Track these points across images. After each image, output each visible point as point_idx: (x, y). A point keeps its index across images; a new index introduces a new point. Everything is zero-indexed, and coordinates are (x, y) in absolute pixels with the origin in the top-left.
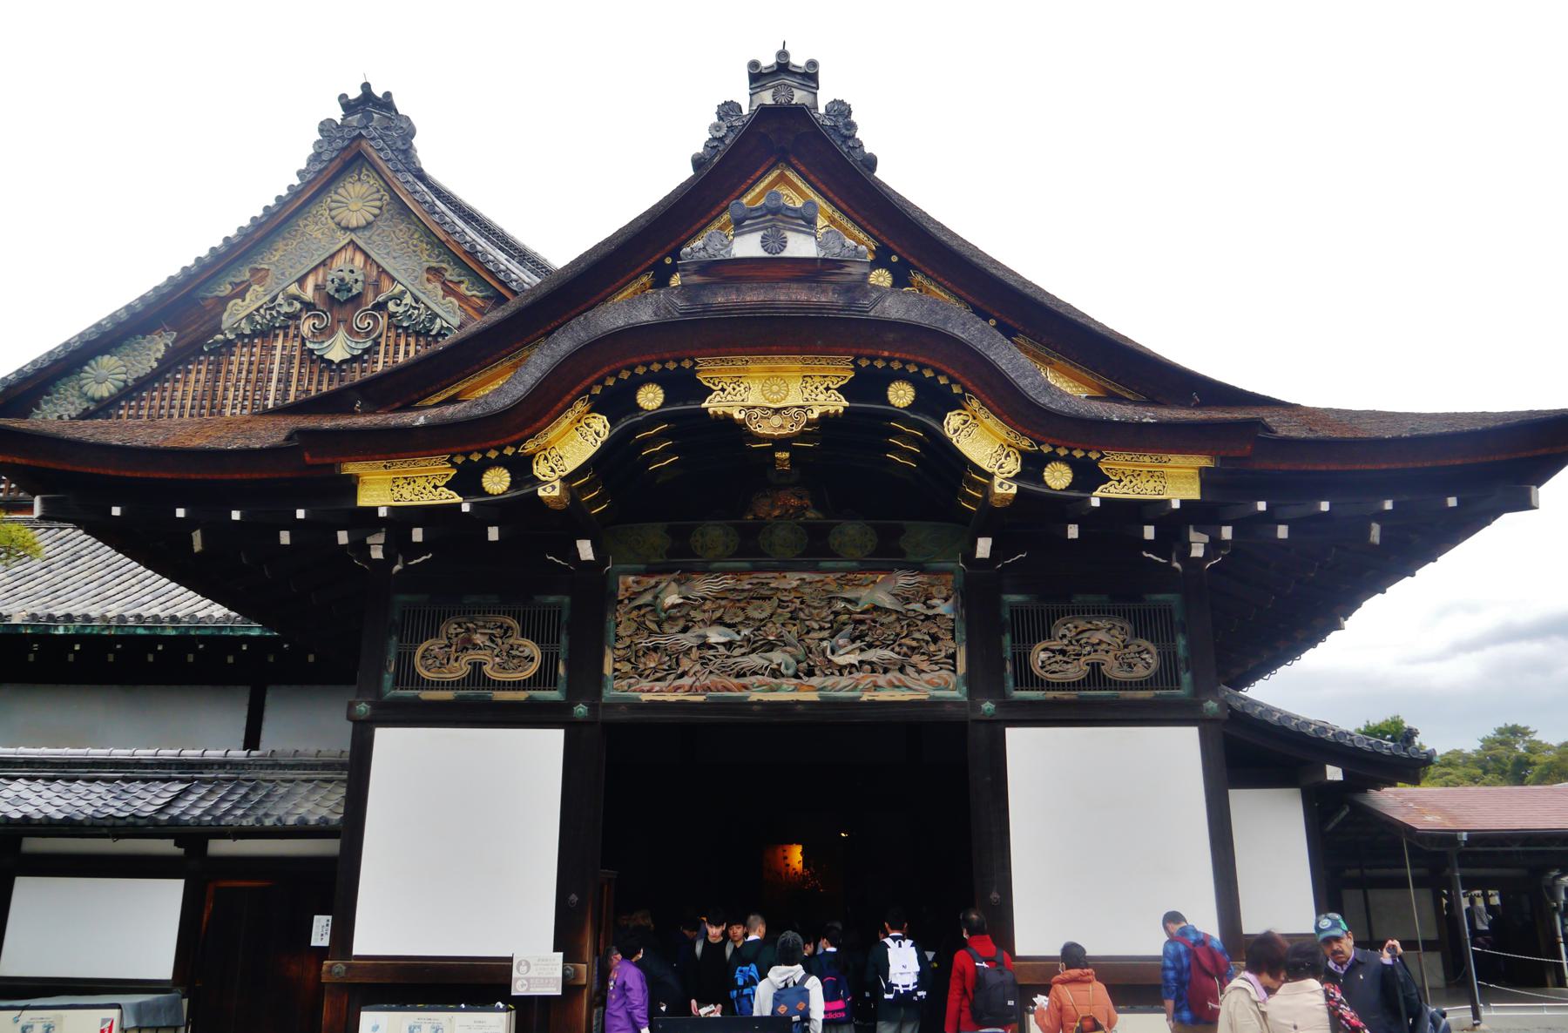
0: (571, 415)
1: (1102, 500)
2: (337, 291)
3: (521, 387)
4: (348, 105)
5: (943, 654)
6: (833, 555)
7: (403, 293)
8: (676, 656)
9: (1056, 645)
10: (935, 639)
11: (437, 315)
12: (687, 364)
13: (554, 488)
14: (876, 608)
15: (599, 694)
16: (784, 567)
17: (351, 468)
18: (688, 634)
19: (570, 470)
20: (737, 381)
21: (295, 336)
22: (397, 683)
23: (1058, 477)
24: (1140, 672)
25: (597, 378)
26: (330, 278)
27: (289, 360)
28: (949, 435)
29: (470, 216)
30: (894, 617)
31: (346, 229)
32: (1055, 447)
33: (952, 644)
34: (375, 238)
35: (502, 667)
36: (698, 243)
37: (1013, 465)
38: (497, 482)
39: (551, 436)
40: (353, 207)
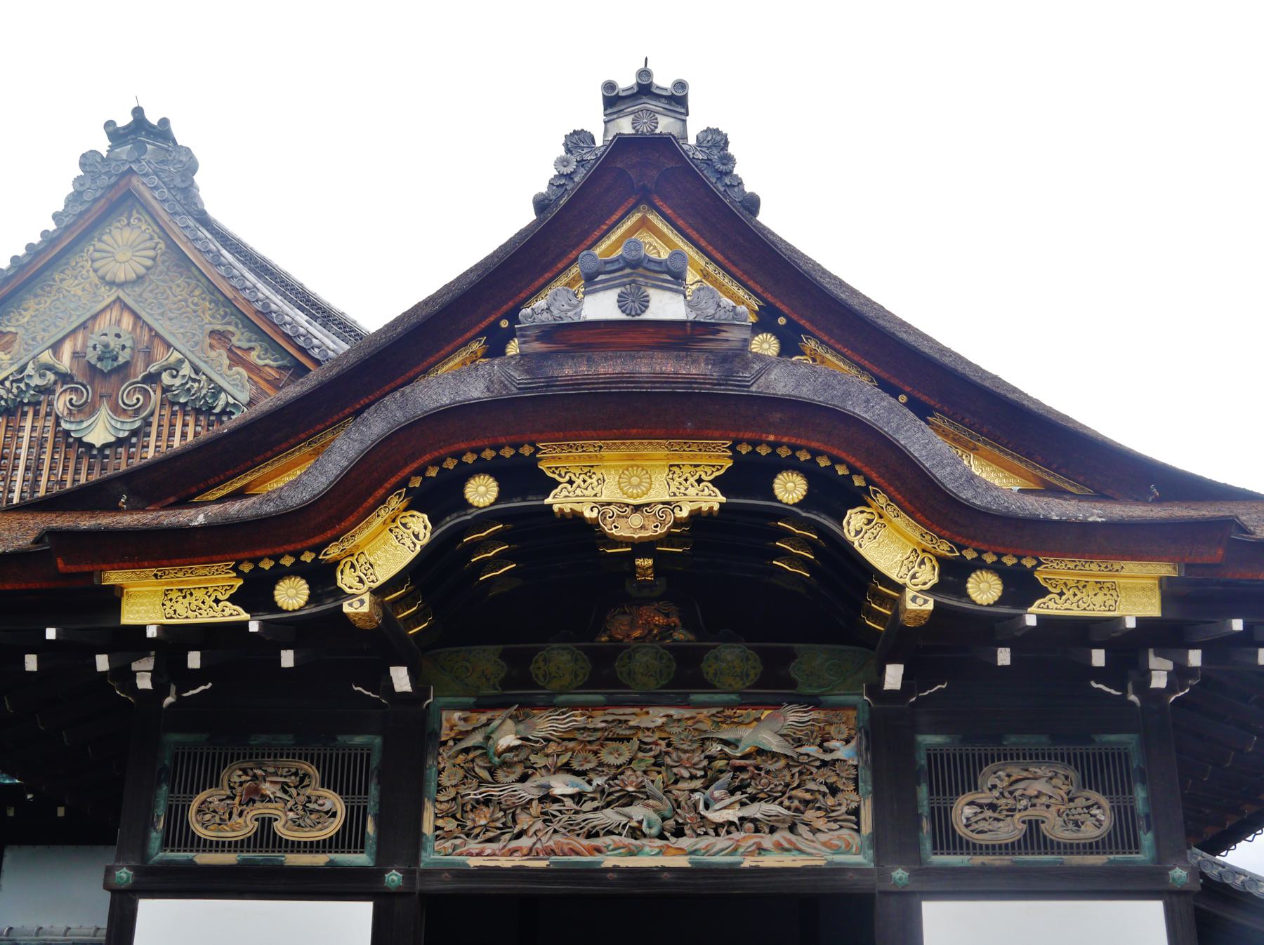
0: (384, 513)
1: (1040, 618)
2: (100, 359)
3: (323, 479)
5: (844, 809)
6: (706, 685)
7: (181, 362)
8: (512, 811)
9: (985, 797)
10: (834, 790)
11: (221, 389)
12: (526, 451)
13: (362, 602)
14: (760, 752)
15: (416, 858)
16: (645, 702)
17: (113, 578)
18: (528, 784)
19: (382, 580)
20: (589, 471)
21: (48, 414)
22: (166, 844)
23: (984, 590)
24: (1090, 832)
25: (415, 467)
26: (91, 343)
28: (850, 536)
29: (263, 269)
30: (782, 763)
31: (112, 284)
32: (980, 552)
33: (854, 796)
34: (146, 295)
35: (297, 824)
36: (541, 303)
37: (929, 575)
38: (292, 595)
39: (359, 539)
40: (120, 257)
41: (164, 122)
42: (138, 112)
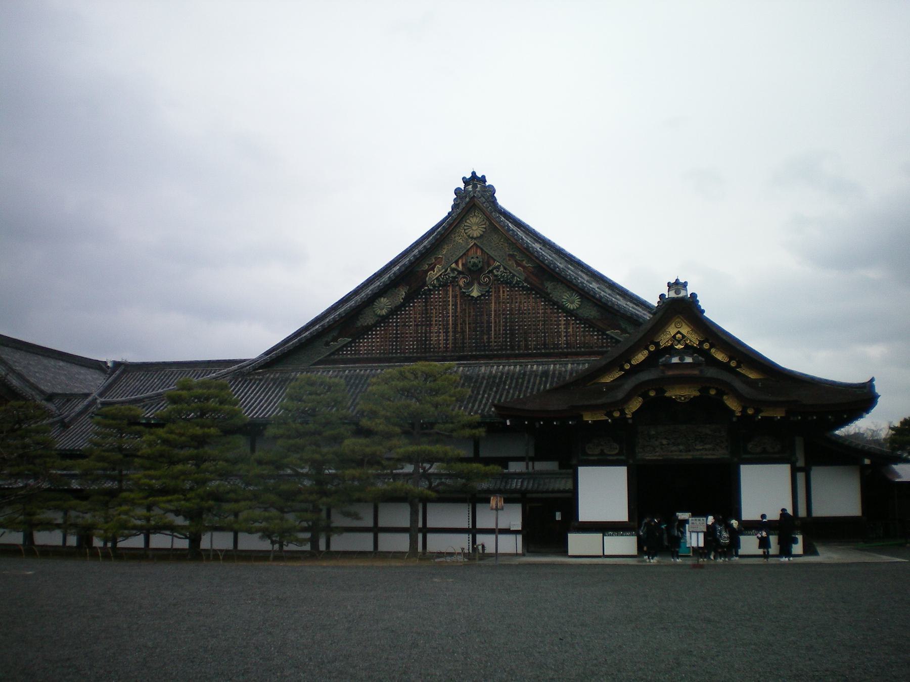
4: (466, 181)
11: (514, 276)
27: (455, 296)
31: (472, 238)
41: (484, 177)
42: (474, 173)
